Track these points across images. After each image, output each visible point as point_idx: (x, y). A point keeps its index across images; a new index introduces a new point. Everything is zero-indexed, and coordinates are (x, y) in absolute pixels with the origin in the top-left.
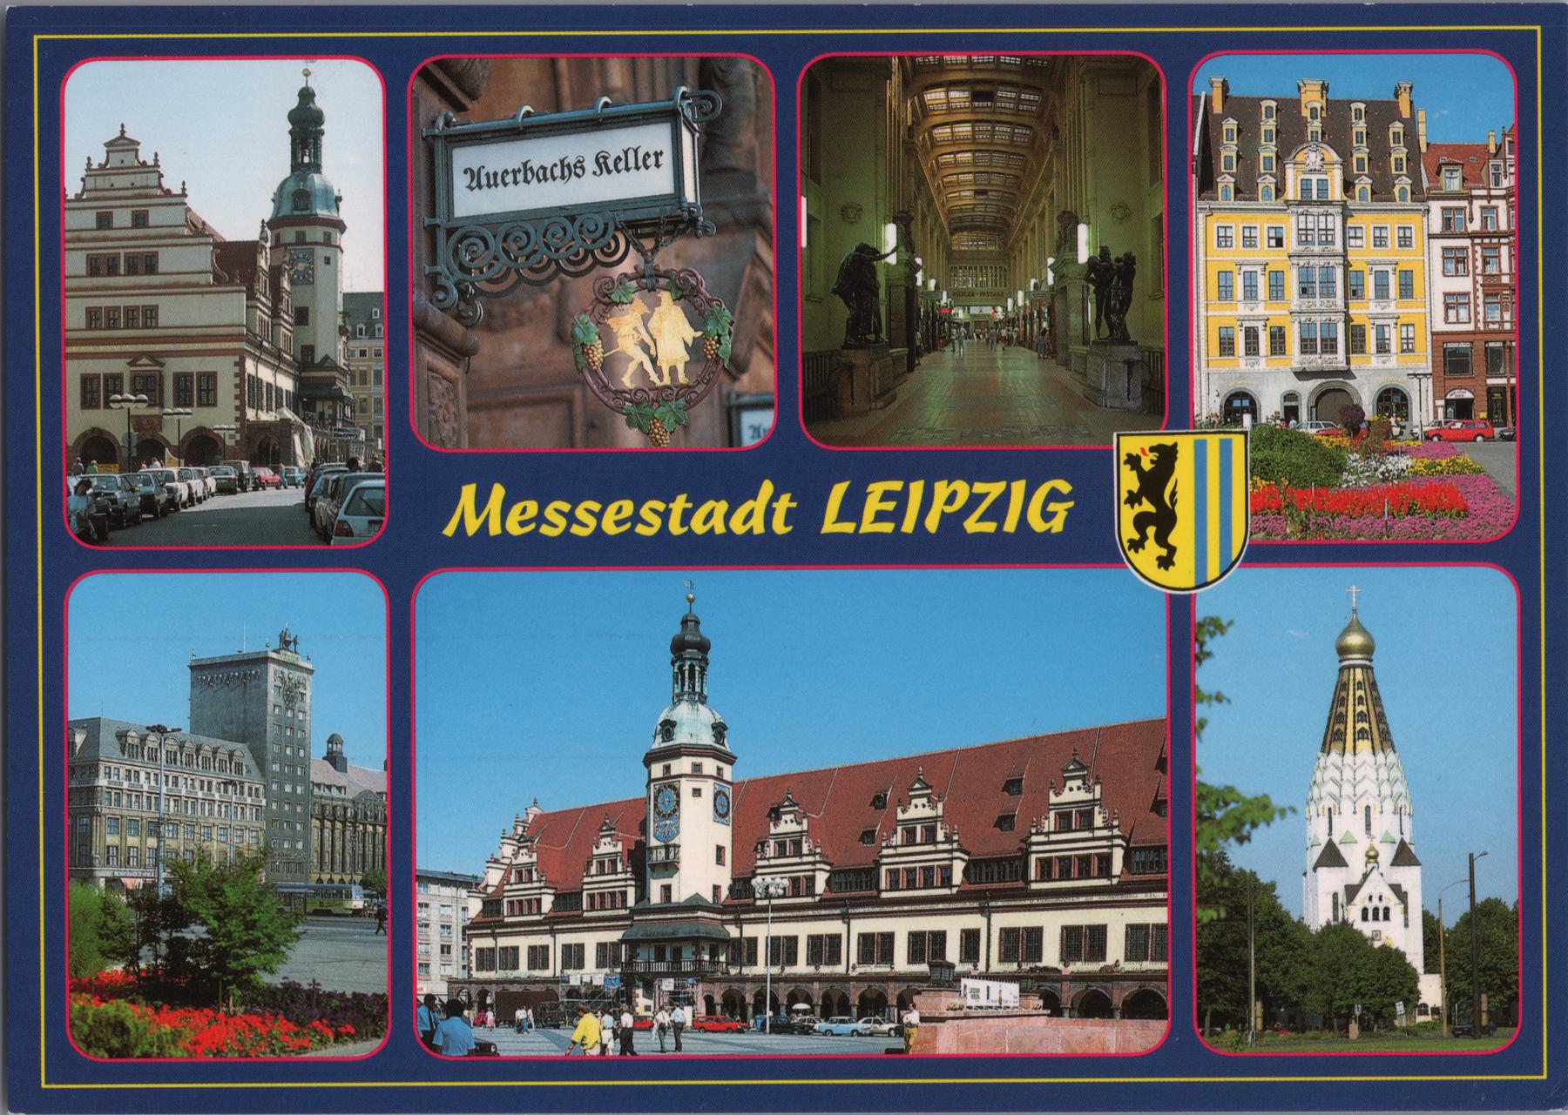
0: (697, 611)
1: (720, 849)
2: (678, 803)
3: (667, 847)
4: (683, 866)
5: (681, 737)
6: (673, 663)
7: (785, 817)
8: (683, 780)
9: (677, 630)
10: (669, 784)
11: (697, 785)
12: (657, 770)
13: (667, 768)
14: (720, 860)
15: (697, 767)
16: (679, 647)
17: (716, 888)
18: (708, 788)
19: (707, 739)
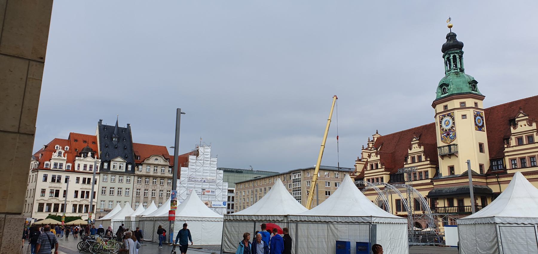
0: (453, 30)
1: (481, 145)
2: (454, 123)
3: (449, 146)
4: (460, 154)
5: (452, 89)
6: (444, 57)
7: (520, 123)
8: (456, 111)
9: (445, 41)
10: (448, 113)
11: (464, 112)
12: (440, 108)
13: (446, 107)
14: (481, 150)
15: (463, 103)
16: (445, 49)
17: (481, 166)
18: (470, 114)
19: (467, 89)
